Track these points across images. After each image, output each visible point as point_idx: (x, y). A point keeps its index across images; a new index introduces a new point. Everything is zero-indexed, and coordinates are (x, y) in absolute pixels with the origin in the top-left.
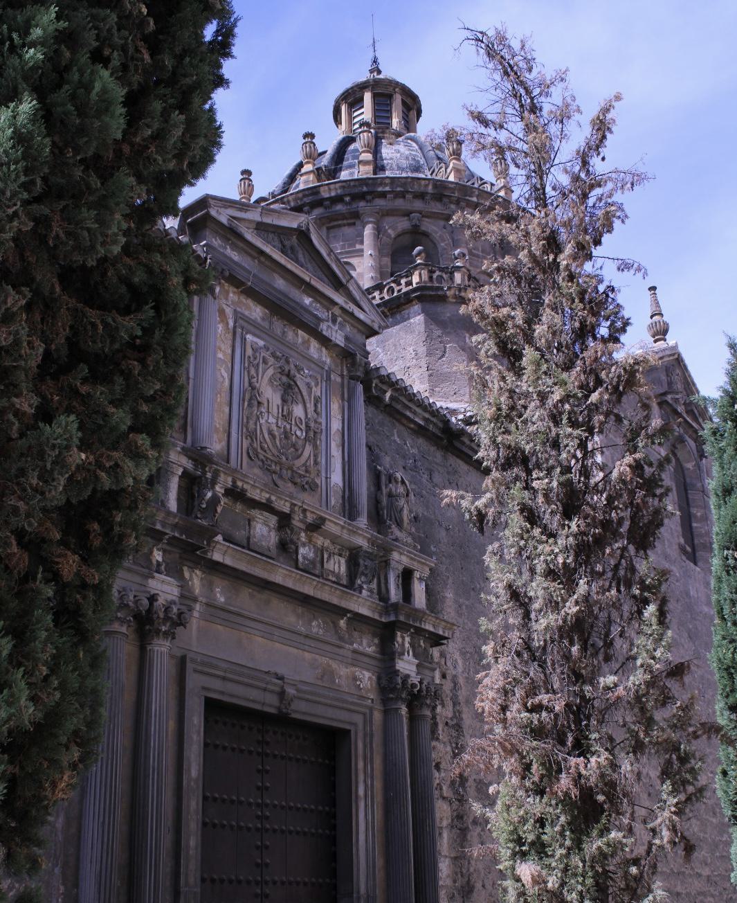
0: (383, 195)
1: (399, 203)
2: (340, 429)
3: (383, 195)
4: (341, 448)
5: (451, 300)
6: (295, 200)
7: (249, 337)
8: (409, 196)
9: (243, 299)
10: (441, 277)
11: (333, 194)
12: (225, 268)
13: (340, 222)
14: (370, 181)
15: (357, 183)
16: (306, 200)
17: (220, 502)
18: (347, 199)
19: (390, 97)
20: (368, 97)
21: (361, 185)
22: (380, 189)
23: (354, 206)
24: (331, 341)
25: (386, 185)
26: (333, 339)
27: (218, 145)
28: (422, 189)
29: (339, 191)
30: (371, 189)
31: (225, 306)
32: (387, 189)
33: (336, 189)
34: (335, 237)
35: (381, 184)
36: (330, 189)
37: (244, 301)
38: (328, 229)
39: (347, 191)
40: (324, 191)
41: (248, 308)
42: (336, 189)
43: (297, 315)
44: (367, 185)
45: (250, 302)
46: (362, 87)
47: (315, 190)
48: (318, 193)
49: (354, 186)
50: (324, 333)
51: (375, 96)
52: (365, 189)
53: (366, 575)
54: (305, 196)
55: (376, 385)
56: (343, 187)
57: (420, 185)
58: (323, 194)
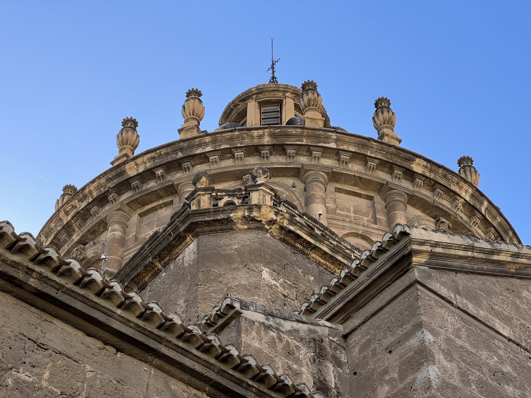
0: (204, 158)
1: (227, 164)
3: (204, 158)
5: (240, 226)
6: (97, 188)
8: (239, 154)
10: (232, 203)
11: (141, 169)
13: (155, 204)
14: (185, 144)
15: (169, 150)
16: (111, 185)
18: (159, 172)
19: (280, 103)
20: (252, 108)
21: (175, 152)
22: (198, 152)
23: (169, 178)
25: (206, 144)
27: (70, 185)
28: (256, 142)
29: (149, 165)
30: (187, 153)
32: (209, 149)
33: (144, 163)
34: (148, 224)
35: (200, 145)
36: (137, 165)
38: (141, 215)
39: (158, 162)
40: (131, 169)
42: (144, 163)
44: (181, 150)
46: (245, 98)
47: (119, 170)
48: (123, 172)
49: (167, 154)
51: (262, 104)
52: (180, 155)
54: (109, 180)
56: (154, 158)
57: (252, 137)
58: (129, 173)
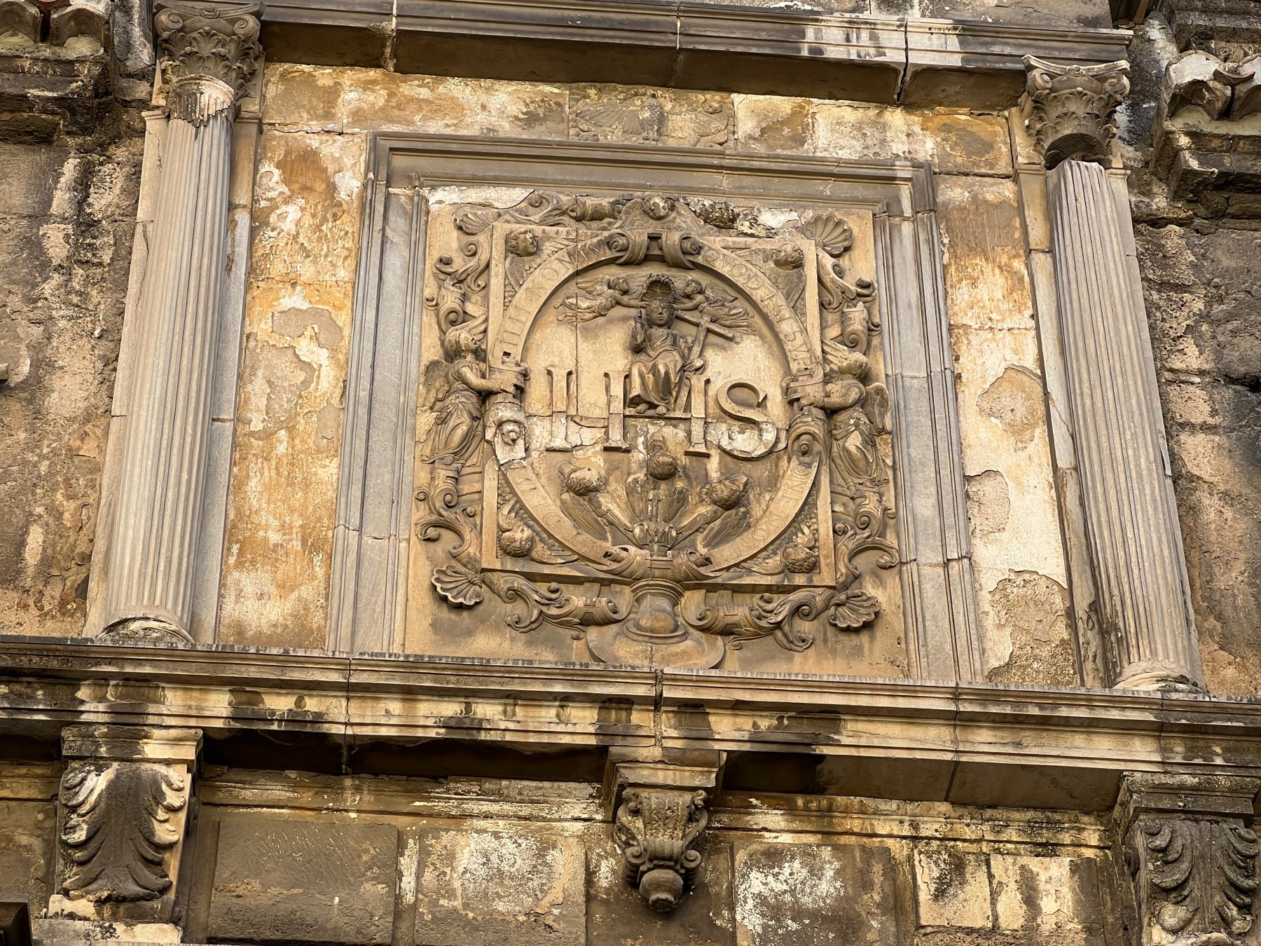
2: (1030, 362)
4: (1040, 431)
7: (444, 198)
9: (416, 88)
12: (233, 12)
17: (158, 797)
24: (886, 70)
26: (894, 56)
31: (314, 142)
37: (424, 93)
41: (436, 108)
43: (678, 42)
45: (455, 88)
50: (832, 53)
53: (1176, 893)
55: (1193, 134)
